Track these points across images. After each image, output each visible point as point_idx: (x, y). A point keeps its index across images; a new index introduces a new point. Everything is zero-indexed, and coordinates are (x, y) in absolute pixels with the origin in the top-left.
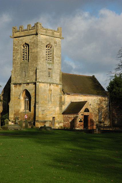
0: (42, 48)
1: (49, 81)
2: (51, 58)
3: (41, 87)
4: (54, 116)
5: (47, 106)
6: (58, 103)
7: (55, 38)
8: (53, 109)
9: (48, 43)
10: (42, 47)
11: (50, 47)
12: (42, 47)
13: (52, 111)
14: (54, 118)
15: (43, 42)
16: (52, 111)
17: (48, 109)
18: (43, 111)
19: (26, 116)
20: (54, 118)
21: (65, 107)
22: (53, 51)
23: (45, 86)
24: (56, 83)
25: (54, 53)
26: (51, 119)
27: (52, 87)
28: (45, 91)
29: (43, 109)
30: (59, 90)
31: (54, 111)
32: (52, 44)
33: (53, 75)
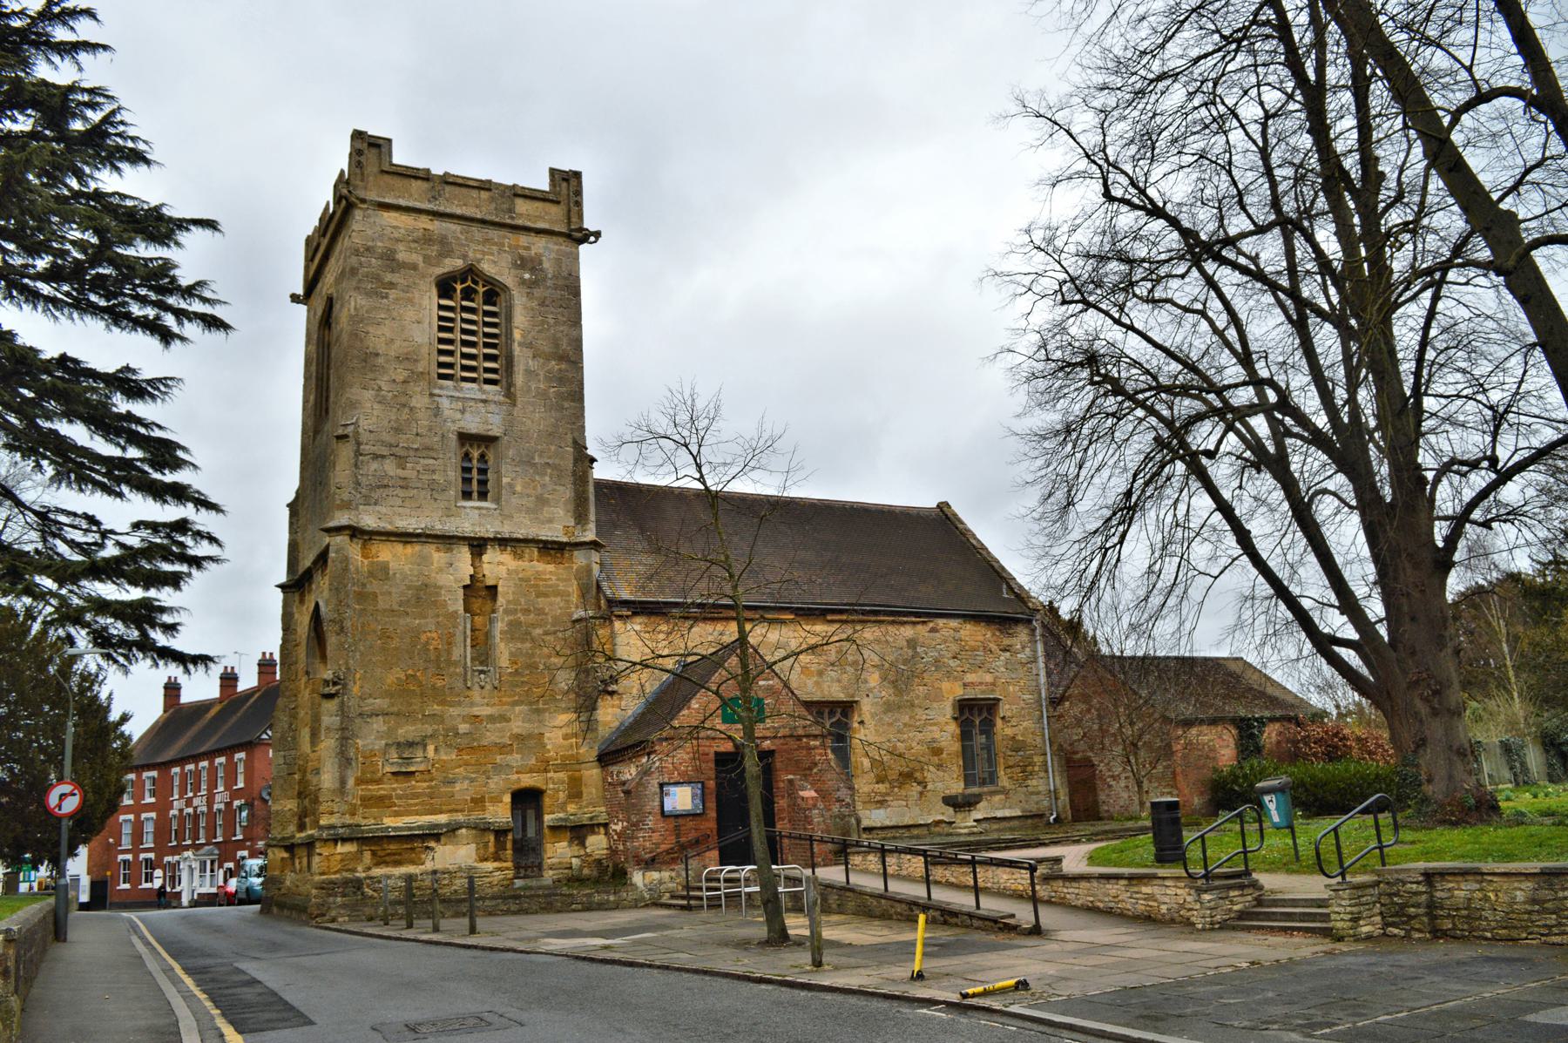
0: (393, 294)
1: (472, 519)
2: (488, 357)
3: (385, 568)
4: (527, 781)
5: (454, 711)
6: (565, 679)
7: (523, 239)
8: (517, 726)
9: (454, 264)
10: (392, 285)
11: (481, 290)
12: (392, 285)
13: (503, 748)
14: (527, 800)
15: (402, 255)
16: (503, 748)
17: (463, 728)
18: (411, 744)
19: (63, 797)
20: (527, 800)
21: (612, 715)
22: (509, 318)
23: (424, 560)
24: (546, 533)
25: (517, 335)
26: (501, 813)
27: (497, 565)
28: (424, 595)
29: (407, 731)
30: (573, 588)
31: (529, 741)
32: (496, 266)
33: (505, 480)
